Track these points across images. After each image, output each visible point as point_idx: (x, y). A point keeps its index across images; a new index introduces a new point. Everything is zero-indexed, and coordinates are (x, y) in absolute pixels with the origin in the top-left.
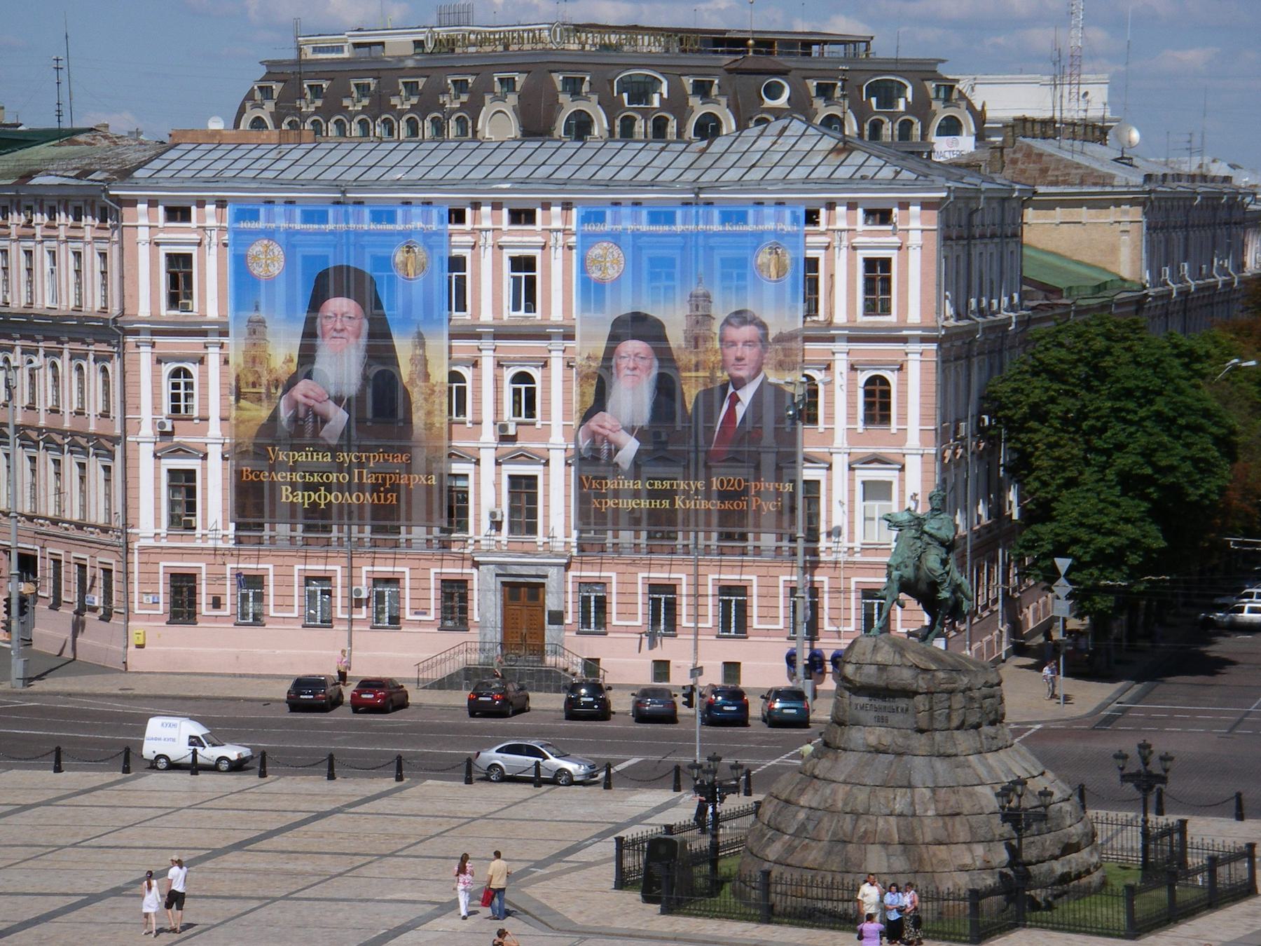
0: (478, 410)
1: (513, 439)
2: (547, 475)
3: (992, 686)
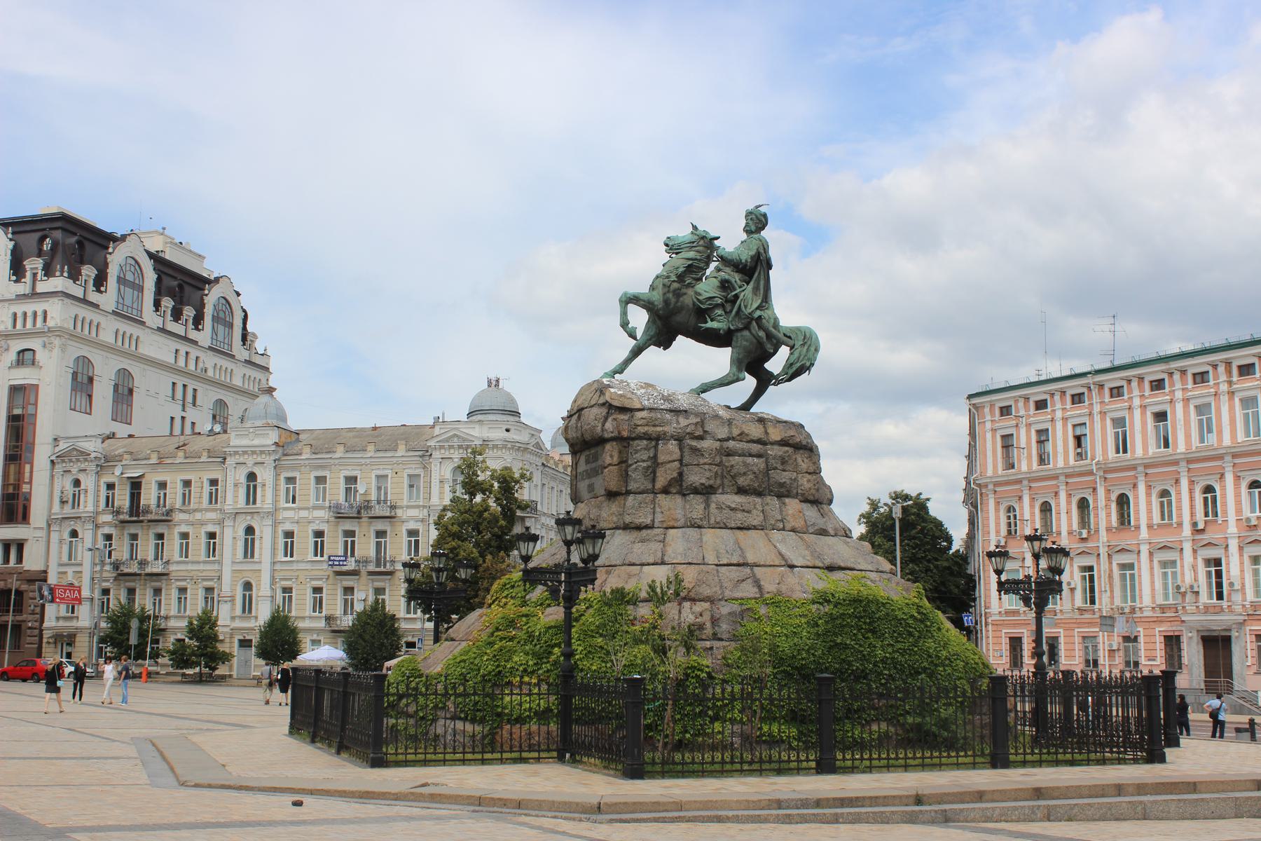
0: (1180, 516)
1: (1202, 531)
2: (1227, 557)
3: (759, 441)
